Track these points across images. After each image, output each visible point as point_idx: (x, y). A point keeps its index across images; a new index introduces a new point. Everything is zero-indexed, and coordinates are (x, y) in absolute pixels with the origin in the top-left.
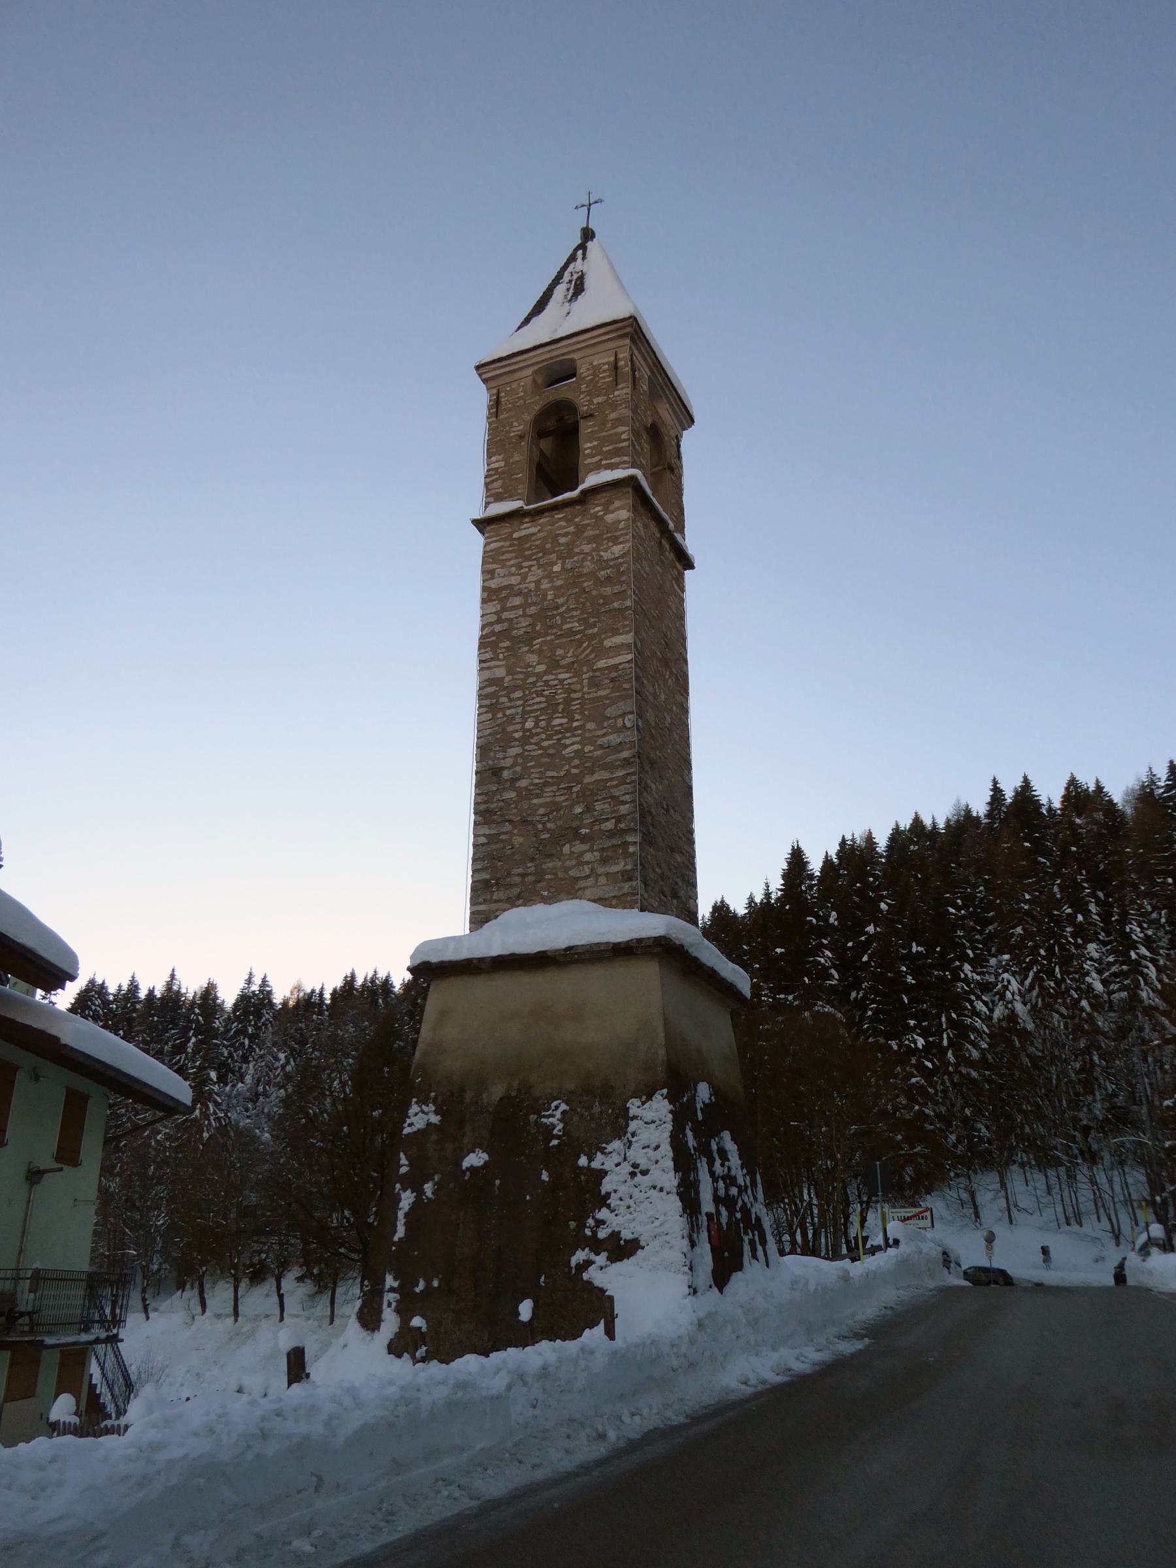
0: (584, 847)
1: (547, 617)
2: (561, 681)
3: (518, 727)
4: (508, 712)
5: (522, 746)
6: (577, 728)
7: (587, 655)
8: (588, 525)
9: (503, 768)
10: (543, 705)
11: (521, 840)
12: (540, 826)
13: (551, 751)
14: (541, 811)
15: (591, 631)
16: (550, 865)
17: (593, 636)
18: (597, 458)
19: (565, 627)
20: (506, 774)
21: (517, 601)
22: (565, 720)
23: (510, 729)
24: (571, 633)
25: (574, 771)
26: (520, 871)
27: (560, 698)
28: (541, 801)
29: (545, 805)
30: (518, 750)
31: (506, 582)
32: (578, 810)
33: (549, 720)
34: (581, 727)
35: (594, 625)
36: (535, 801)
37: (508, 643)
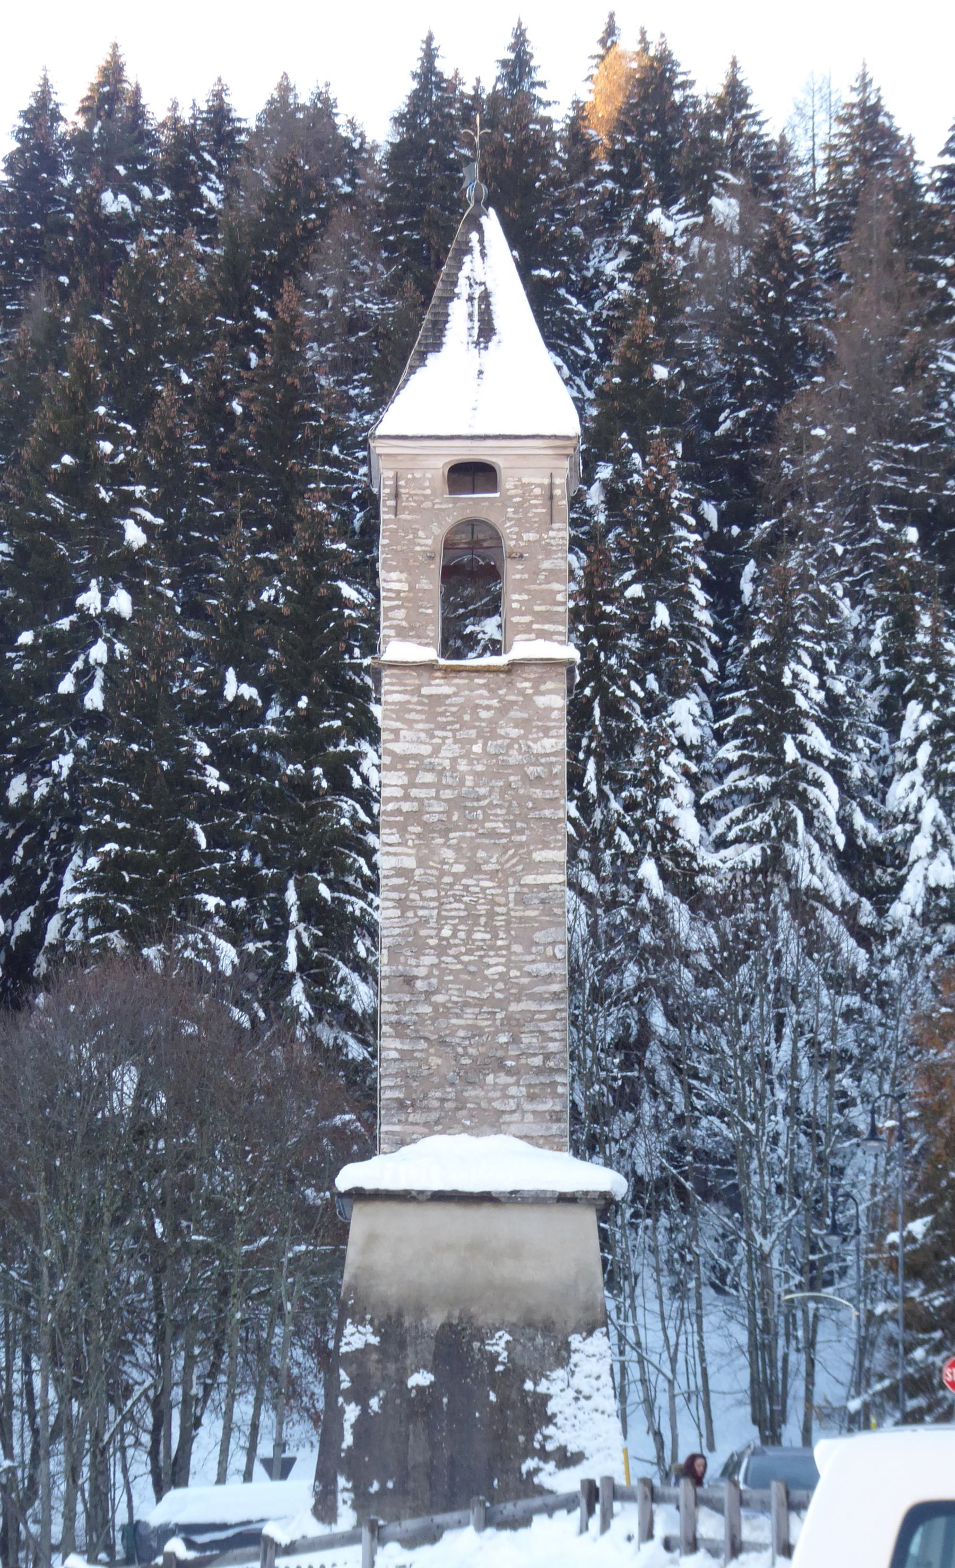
0: (511, 1080)
2: (484, 890)
4: (421, 913)
6: (501, 948)
8: (515, 703)
9: (416, 978)
10: (463, 914)
11: (439, 1061)
12: (460, 1050)
14: (461, 1033)
17: (521, 845)
18: (527, 619)
20: (420, 985)
21: (429, 778)
22: (488, 936)
23: (423, 933)
24: (493, 834)
25: (498, 995)
27: (482, 909)
29: (467, 1027)
31: (413, 749)
33: (469, 933)
34: (508, 947)
35: (521, 832)
36: (454, 1021)
37: (418, 829)
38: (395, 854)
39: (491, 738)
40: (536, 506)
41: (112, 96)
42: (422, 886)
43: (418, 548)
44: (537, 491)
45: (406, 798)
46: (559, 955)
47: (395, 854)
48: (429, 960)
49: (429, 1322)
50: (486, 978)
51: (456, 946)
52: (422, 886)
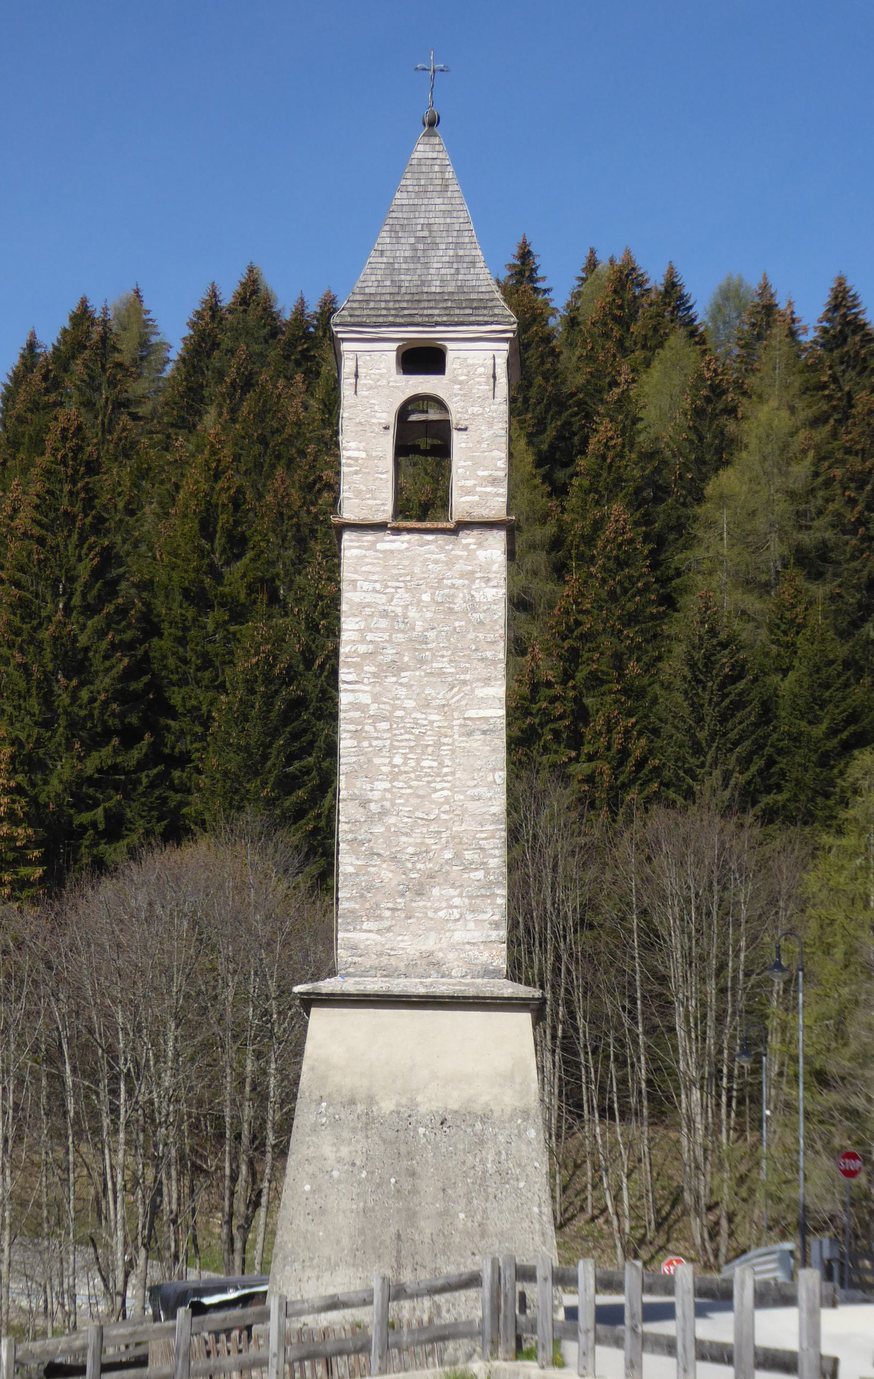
0: (453, 892)
1: (416, 650)
3: (387, 761)
4: (375, 743)
5: (391, 781)
6: (446, 775)
7: (458, 701)
8: (461, 557)
9: (370, 801)
10: (412, 744)
11: (391, 875)
12: (409, 865)
13: (421, 792)
14: (411, 850)
15: (462, 677)
16: (421, 904)
17: (464, 682)
18: (471, 483)
19: (435, 665)
20: (373, 807)
21: (384, 623)
22: (435, 764)
23: (376, 761)
24: (441, 673)
25: (444, 816)
26: (390, 905)
27: (429, 740)
28: (411, 840)
29: (416, 845)
30: (387, 785)
31: (369, 598)
32: (448, 855)
33: (418, 761)
34: (453, 773)
35: (466, 671)
36: (404, 839)
37: (373, 669)
38: (352, 691)
39: (437, 588)
40: (479, 384)
41: (252, 292)
42: (377, 718)
43: (374, 421)
44: (481, 370)
45: (363, 641)
46: (499, 781)
47: (352, 691)
49: (380, 1109)
50: (432, 802)
51: (406, 772)
52: (377, 718)
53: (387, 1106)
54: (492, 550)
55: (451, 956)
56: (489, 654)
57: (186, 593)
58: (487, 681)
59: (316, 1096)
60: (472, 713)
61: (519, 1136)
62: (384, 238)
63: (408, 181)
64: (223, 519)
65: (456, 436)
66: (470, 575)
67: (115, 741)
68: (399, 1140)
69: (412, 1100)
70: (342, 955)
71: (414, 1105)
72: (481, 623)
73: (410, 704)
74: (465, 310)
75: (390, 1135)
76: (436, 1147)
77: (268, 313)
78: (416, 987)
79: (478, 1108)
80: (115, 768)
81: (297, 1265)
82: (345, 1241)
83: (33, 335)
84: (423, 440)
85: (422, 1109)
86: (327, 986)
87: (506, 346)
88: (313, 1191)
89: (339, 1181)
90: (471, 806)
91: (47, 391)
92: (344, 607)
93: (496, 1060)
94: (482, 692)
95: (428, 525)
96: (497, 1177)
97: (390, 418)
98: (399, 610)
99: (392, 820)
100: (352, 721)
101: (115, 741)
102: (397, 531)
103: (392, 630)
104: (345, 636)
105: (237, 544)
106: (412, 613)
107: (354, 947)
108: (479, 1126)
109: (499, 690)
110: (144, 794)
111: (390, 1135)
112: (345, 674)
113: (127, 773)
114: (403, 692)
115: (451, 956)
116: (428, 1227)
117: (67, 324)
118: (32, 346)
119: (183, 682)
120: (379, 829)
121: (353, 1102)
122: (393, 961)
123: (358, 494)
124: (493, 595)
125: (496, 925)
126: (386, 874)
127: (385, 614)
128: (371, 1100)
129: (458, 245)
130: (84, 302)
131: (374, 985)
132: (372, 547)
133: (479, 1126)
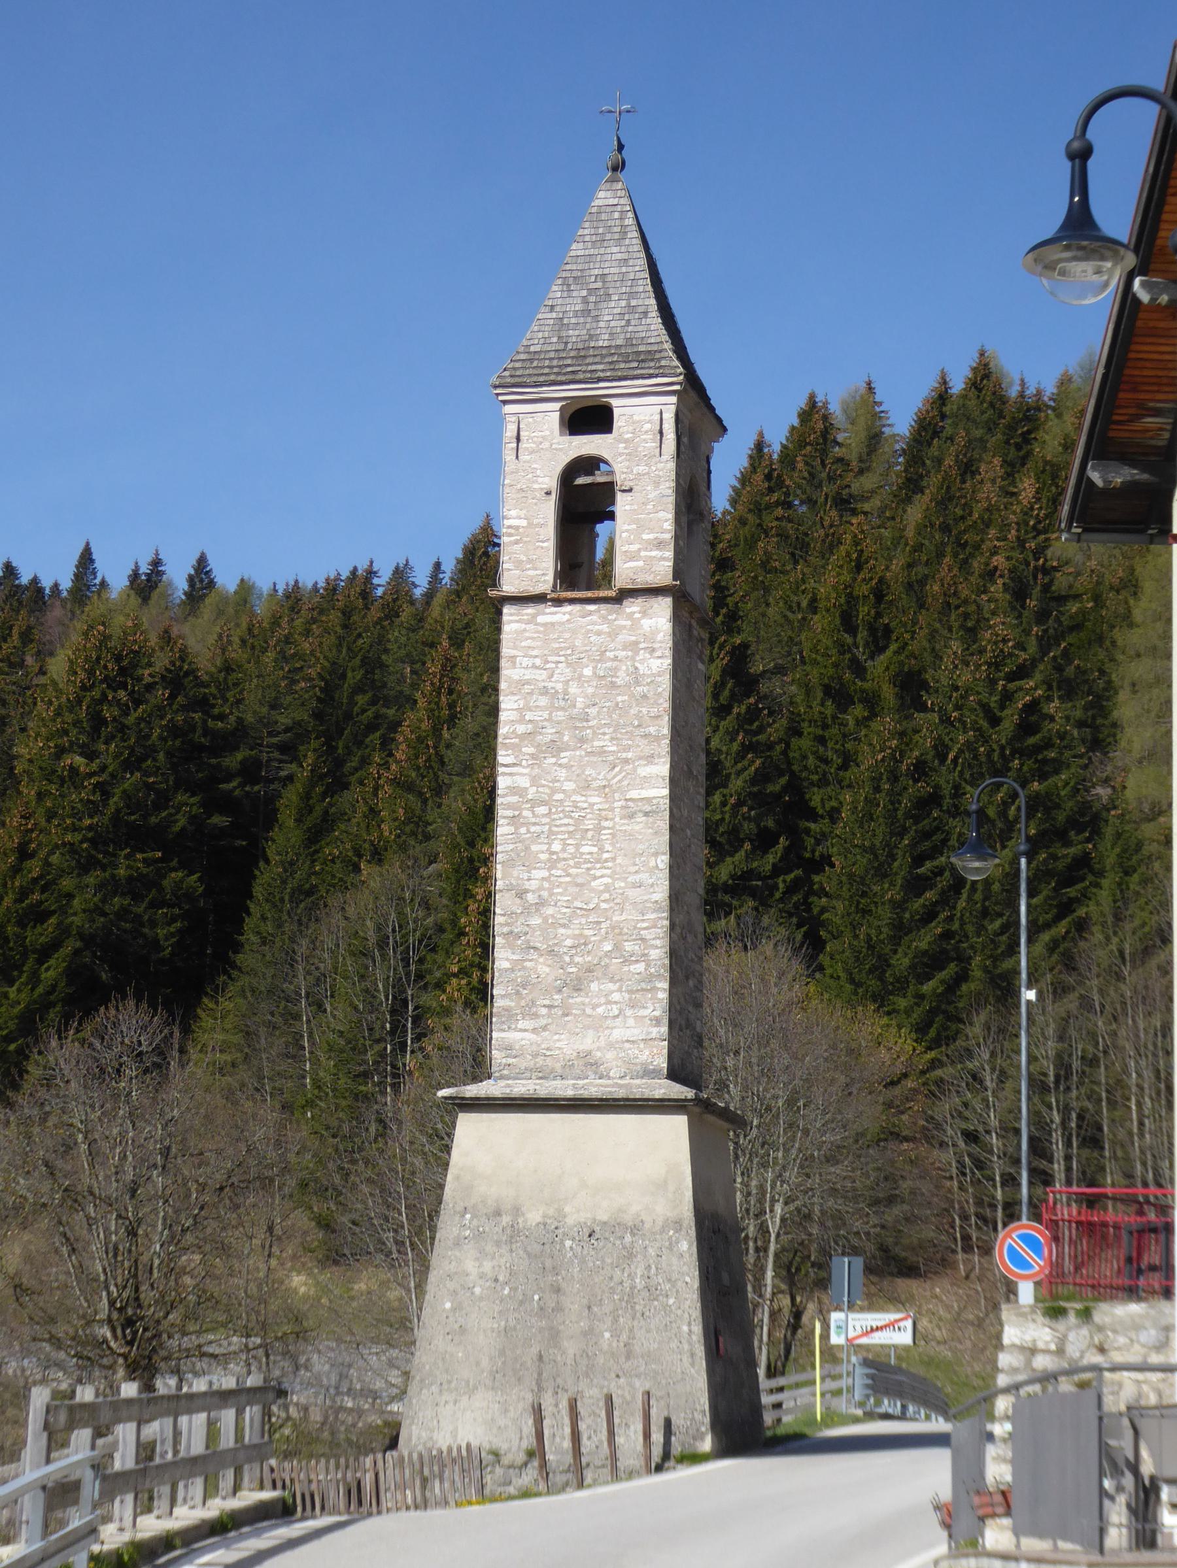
0: (611, 986)
1: (576, 728)
2: (592, 805)
3: (545, 847)
4: (533, 829)
5: (549, 869)
6: (606, 861)
8: (624, 627)
9: (527, 891)
10: (571, 828)
11: (547, 970)
12: (567, 959)
13: (580, 880)
14: (569, 942)
15: (624, 755)
16: (579, 1000)
17: (626, 761)
19: (596, 744)
20: (530, 897)
21: (543, 701)
22: (595, 849)
23: (534, 848)
24: (602, 752)
25: (604, 906)
26: (547, 1002)
27: (589, 824)
28: (569, 932)
29: (575, 937)
30: (545, 874)
31: (529, 675)
32: (607, 947)
33: (578, 846)
34: (614, 859)
35: (627, 749)
36: (562, 931)
37: (531, 750)
38: (511, 774)
39: (599, 661)
41: (984, 376)
42: (534, 803)
43: (536, 486)
44: (647, 426)
45: (522, 720)
46: (661, 866)
47: (511, 774)
48: (538, 874)
49: (525, 1221)
50: (593, 890)
52: (534, 803)
53: (533, 1217)
54: (658, 619)
55: (610, 1055)
56: (652, 730)
57: (827, 690)
58: (650, 759)
59: (459, 1208)
60: (633, 794)
61: (670, 1248)
62: (556, 291)
63: (586, 231)
64: (864, 611)
65: (619, 496)
66: (634, 646)
67: (747, 846)
68: (545, 1254)
69: (560, 1211)
70: (497, 1056)
71: (561, 1215)
72: (645, 697)
73: (569, 786)
74: (631, 362)
75: (537, 1248)
76: (583, 1261)
77: (999, 398)
78: (564, 1089)
79: (628, 1219)
80: (748, 875)
81: (434, 1389)
82: (485, 1362)
83: (761, 434)
84: (584, 504)
85: (570, 1221)
86: (472, 1090)
87: (674, 399)
88: (454, 1309)
89: (481, 1299)
90: (632, 893)
91: (771, 490)
92: (503, 686)
93: (648, 1165)
94: (645, 771)
95: (589, 594)
96: (645, 1294)
97: (551, 481)
98: (559, 687)
99: (550, 911)
100: (509, 806)
101: (747, 846)
102: (558, 602)
103: (552, 708)
104: (503, 716)
105: (880, 638)
106: (573, 689)
107: (509, 1048)
108: (628, 1238)
109: (662, 768)
110: (781, 900)
111: (537, 1248)
112: (503, 756)
113: (763, 879)
114: (562, 774)
115: (610, 1055)
116: (571, 1348)
117: (796, 422)
118: (760, 446)
119: (823, 782)
120: (536, 921)
121: (498, 1213)
122: (549, 1062)
123: (519, 564)
124: (658, 665)
125: (657, 1021)
126: (544, 968)
127: (545, 691)
128: (517, 1211)
129: (632, 295)
130: (812, 397)
131: (521, 1088)
132: (532, 620)
133: (628, 1238)
